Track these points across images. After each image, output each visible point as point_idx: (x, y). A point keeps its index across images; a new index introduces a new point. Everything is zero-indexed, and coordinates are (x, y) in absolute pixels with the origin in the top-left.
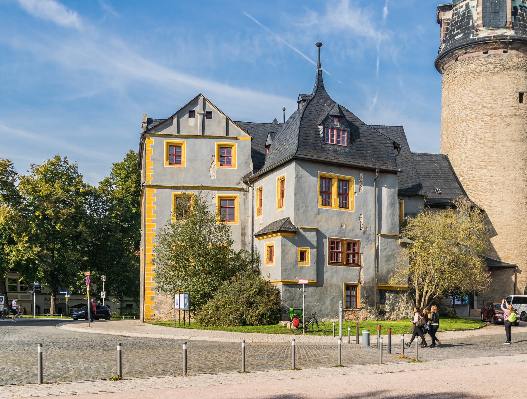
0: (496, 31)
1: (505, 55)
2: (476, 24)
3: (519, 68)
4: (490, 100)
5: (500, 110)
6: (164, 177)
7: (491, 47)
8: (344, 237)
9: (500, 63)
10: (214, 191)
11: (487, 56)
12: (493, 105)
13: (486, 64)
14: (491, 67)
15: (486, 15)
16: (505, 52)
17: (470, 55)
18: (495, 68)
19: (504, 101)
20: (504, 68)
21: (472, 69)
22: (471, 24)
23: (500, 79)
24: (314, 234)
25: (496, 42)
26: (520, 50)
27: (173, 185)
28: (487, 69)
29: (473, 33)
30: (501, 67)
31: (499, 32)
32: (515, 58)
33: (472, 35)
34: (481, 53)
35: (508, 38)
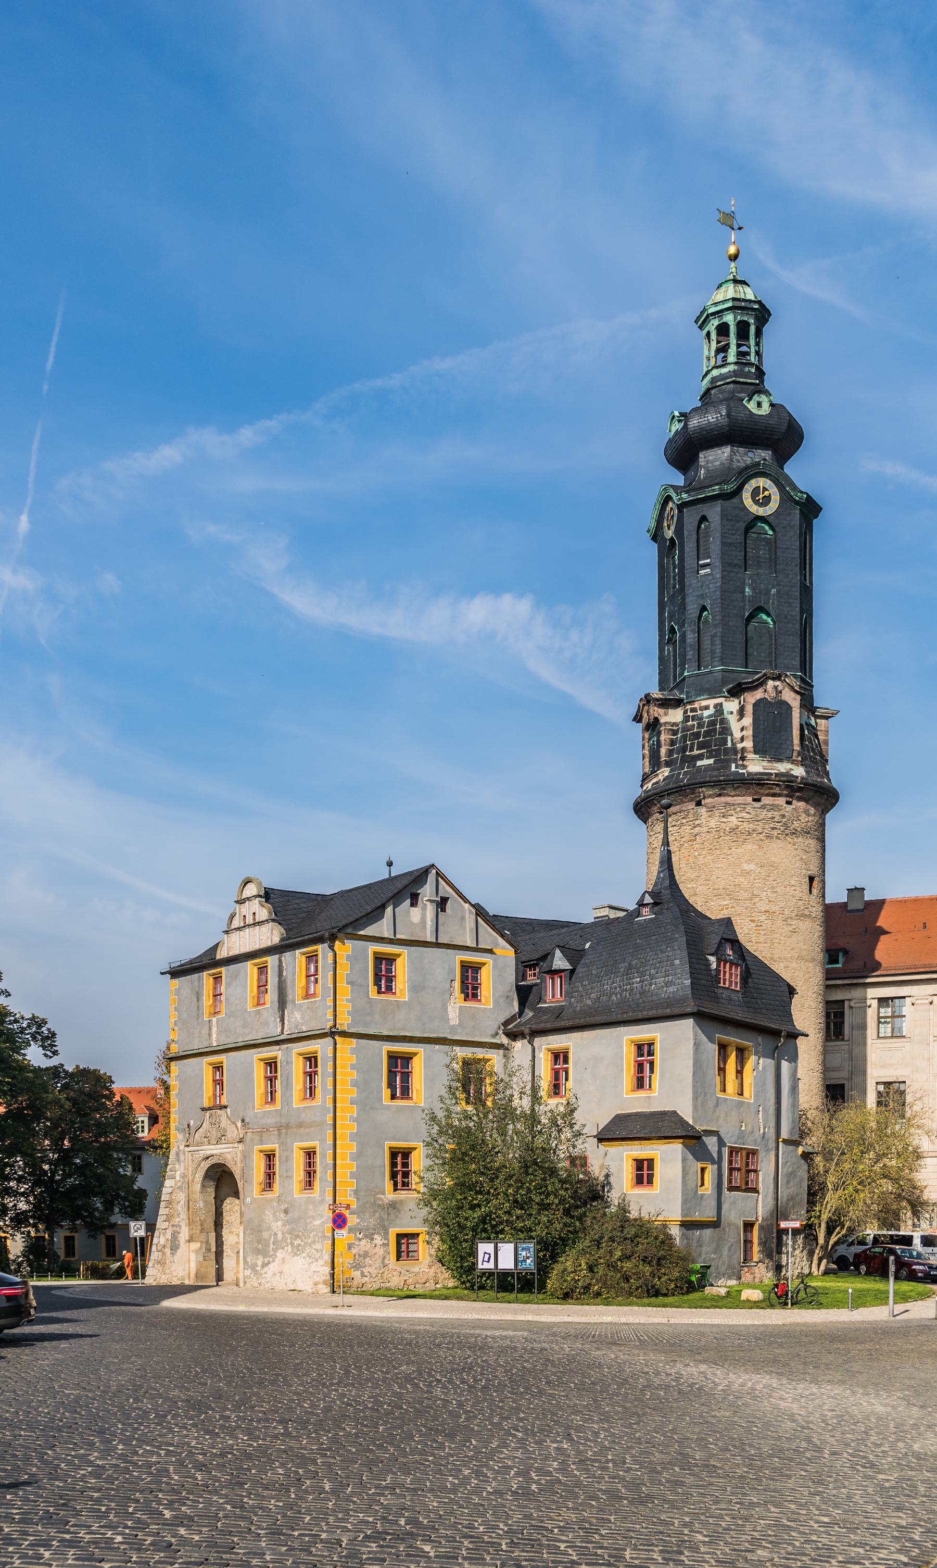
0: (776, 765)
1: (789, 808)
2: (739, 746)
3: (808, 833)
4: (765, 884)
5: (783, 904)
6: (369, 1018)
7: (767, 792)
8: (744, 1144)
9: (781, 822)
10: (454, 1048)
11: (759, 806)
12: (769, 894)
13: (757, 821)
14: (767, 827)
15: (759, 733)
16: (789, 803)
17: (729, 799)
18: (773, 829)
19: (788, 889)
20: (787, 832)
21: (732, 825)
22: (729, 744)
23: (781, 850)
24: (715, 1139)
25: (777, 785)
26: (810, 802)
27: (385, 1033)
28: (760, 830)
29: (735, 761)
30: (782, 828)
31: (783, 767)
32: (804, 815)
33: (733, 765)
34: (749, 799)
35: (799, 780)
